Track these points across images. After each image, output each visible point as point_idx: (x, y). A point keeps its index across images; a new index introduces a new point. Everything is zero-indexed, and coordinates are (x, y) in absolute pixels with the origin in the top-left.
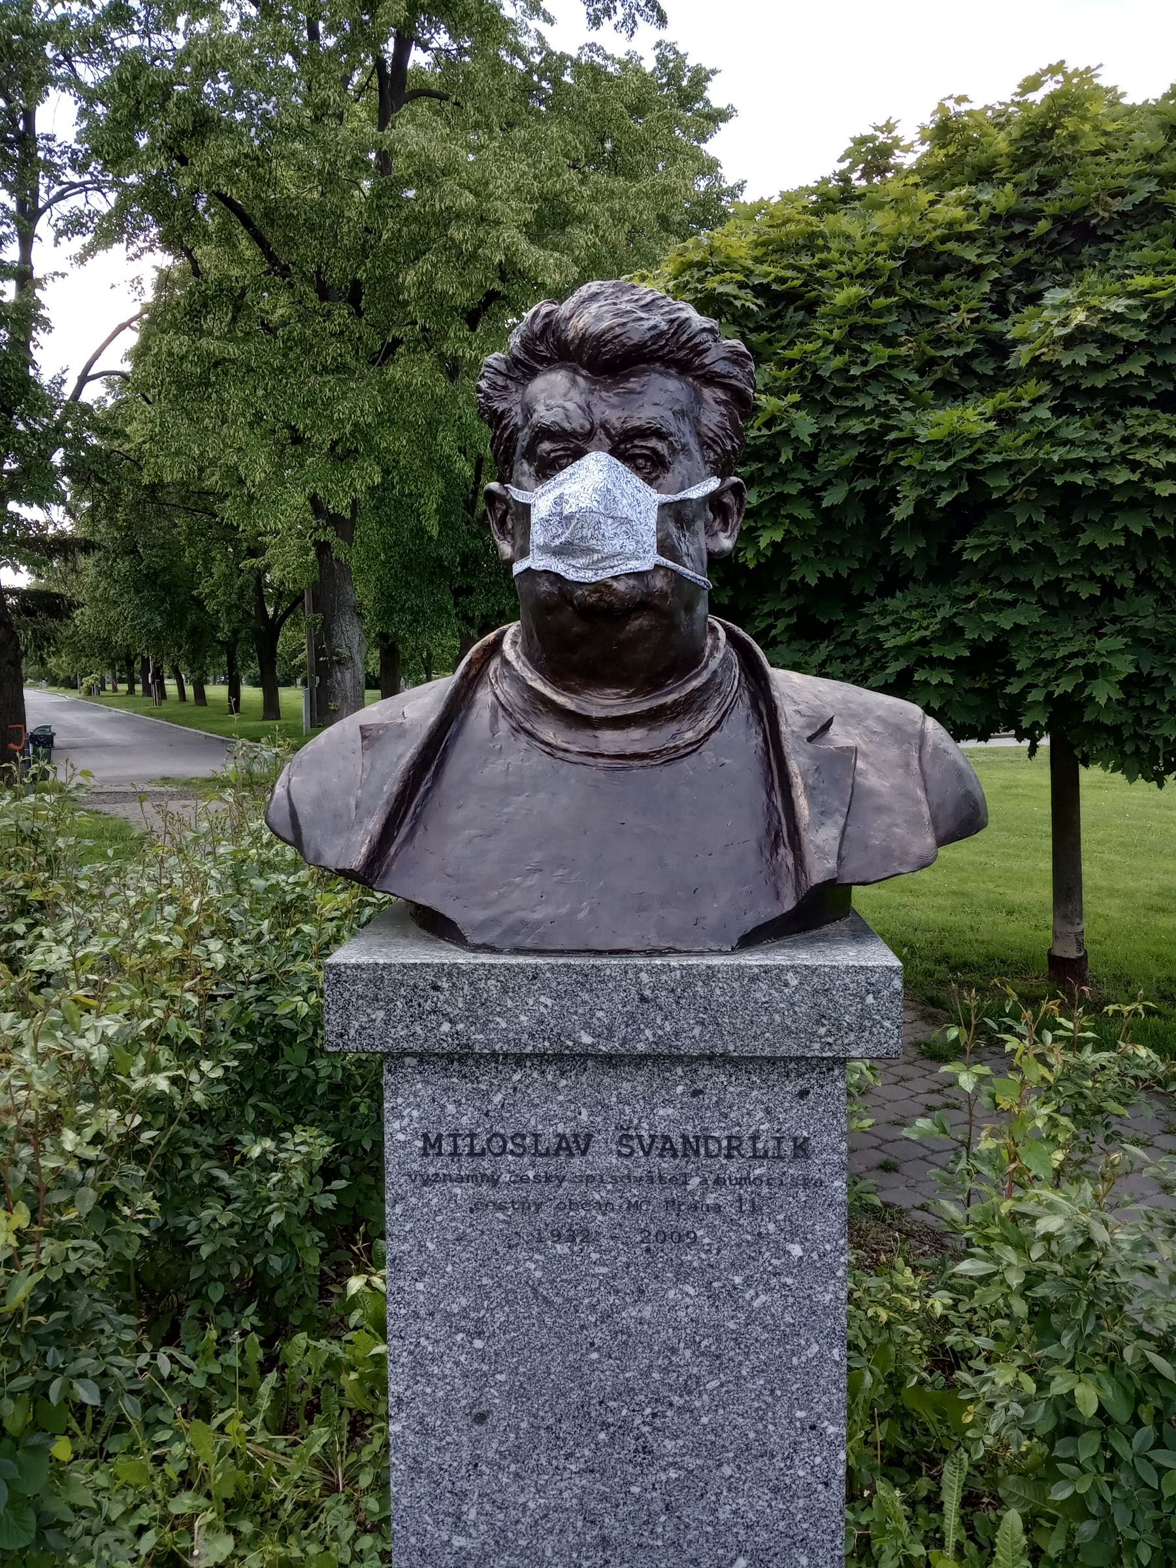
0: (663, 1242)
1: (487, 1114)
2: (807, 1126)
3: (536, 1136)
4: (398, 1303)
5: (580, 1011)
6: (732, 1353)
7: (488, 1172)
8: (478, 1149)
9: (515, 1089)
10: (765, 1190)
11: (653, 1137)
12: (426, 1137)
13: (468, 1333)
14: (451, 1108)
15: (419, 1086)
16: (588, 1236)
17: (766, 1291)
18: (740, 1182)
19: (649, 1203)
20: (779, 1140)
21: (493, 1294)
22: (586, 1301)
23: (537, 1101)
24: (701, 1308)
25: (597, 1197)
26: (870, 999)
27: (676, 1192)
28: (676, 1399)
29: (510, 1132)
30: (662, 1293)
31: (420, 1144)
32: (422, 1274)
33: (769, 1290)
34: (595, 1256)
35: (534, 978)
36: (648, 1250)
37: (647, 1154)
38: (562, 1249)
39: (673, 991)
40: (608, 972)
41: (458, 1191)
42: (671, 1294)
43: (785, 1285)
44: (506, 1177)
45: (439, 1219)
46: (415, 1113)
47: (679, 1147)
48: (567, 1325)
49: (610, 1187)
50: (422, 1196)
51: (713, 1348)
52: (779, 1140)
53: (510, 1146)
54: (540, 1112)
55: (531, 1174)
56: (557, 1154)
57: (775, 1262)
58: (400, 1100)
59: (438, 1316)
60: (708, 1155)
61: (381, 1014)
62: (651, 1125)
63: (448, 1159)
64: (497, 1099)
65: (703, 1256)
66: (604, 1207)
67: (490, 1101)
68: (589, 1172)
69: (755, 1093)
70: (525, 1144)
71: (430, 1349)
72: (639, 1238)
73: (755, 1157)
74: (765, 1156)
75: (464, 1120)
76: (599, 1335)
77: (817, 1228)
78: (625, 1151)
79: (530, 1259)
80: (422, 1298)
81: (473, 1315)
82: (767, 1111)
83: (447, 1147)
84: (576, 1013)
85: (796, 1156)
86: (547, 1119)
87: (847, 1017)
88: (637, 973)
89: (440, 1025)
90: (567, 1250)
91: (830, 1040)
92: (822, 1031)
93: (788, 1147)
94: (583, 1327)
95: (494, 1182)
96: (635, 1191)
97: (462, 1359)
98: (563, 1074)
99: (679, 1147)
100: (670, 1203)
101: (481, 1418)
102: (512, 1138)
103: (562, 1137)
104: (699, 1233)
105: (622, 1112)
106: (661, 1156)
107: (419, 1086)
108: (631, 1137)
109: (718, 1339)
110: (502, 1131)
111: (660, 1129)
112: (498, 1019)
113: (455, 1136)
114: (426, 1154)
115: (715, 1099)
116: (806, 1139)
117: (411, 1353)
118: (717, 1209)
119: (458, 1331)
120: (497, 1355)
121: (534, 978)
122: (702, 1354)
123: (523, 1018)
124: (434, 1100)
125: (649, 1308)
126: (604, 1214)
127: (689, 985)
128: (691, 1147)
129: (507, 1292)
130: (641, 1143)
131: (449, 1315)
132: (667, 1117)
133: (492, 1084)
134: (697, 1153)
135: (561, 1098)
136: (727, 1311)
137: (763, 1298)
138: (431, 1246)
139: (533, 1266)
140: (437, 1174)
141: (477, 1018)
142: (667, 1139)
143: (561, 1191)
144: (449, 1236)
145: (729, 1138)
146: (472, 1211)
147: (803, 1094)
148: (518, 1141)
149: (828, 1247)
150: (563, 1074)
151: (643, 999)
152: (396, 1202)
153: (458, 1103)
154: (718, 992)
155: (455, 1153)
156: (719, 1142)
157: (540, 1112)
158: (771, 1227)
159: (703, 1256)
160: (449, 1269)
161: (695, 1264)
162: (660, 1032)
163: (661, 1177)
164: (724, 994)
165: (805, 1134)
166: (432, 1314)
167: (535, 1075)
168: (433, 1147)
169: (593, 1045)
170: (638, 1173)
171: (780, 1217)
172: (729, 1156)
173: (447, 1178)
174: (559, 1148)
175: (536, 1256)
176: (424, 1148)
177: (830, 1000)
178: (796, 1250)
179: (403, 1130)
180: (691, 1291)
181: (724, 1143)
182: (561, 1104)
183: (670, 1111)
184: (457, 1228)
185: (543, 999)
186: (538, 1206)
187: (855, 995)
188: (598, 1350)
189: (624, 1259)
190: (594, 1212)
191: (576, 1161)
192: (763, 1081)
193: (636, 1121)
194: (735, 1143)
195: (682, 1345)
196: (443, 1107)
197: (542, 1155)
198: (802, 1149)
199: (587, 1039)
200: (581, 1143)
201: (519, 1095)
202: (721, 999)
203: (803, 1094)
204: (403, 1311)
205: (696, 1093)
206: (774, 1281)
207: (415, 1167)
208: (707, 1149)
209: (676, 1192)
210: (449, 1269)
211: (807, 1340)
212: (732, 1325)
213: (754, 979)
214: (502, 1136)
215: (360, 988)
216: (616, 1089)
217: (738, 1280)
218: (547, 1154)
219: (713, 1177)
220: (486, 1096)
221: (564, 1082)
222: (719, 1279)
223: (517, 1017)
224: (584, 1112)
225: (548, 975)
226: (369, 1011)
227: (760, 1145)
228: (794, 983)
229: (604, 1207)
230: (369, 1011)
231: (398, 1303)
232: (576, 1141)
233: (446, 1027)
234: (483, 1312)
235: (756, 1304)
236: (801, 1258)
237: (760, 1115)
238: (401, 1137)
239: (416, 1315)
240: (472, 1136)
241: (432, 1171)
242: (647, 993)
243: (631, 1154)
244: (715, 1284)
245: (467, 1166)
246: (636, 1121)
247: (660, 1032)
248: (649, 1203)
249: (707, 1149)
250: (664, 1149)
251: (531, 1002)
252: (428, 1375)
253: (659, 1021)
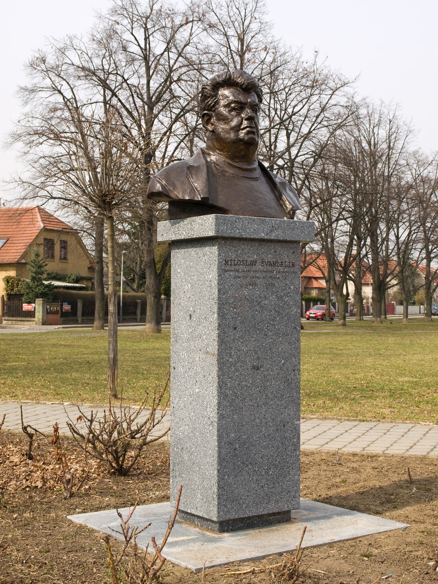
14: (230, 254)
16: (256, 284)
18: (283, 272)
27: (271, 274)
28: (272, 323)
32: (224, 293)
38: (251, 287)
44: (240, 270)
48: (252, 306)
61: (225, 227)
64: (239, 252)
66: (259, 278)
70: (244, 262)
76: (257, 308)
83: (229, 263)
86: (248, 257)
93: (291, 264)
95: (238, 271)
101: (235, 329)
113: (231, 260)
118: (279, 278)
128: (274, 264)
131: (230, 303)
132: (270, 257)
136: (280, 302)
142: (270, 262)
147: (294, 252)
151: (273, 227)
153: (232, 253)
170: (265, 270)
173: (230, 270)
178: (292, 287)
191: (254, 267)
198: (293, 265)
199: (263, 235)
200: (253, 263)
203: (294, 252)
205: (275, 252)
209: (271, 274)
213: (291, 223)
229: (259, 278)
233: (238, 231)
240: (234, 260)
245: (233, 268)
252: (225, 318)
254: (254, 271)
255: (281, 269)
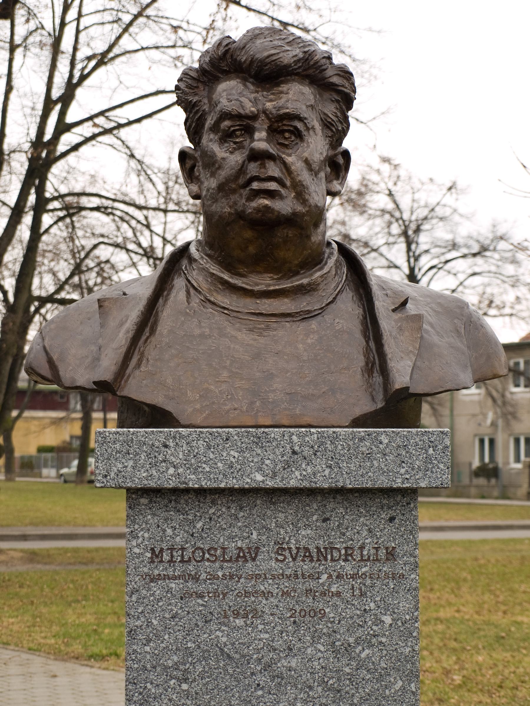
0: (304, 616)
1: (192, 535)
2: (395, 540)
3: (224, 549)
4: (133, 660)
5: (255, 460)
6: (348, 688)
7: (193, 573)
8: (186, 558)
9: (210, 519)
10: (368, 582)
11: (298, 549)
12: (152, 550)
13: (178, 679)
14: (169, 532)
15: (149, 517)
16: (256, 614)
17: (369, 647)
18: (353, 577)
19: (295, 591)
20: (377, 549)
21: (195, 653)
22: (255, 656)
23: (224, 526)
24: (328, 659)
25: (263, 588)
26: (431, 451)
27: (312, 584)
29: (207, 547)
30: (303, 650)
31: (149, 555)
32: (149, 641)
33: (371, 646)
34: (261, 627)
35: (227, 439)
36: (295, 622)
37: (294, 559)
38: (239, 622)
39: (312, 447)
40: (273, 435)
41: (173, 585)
42: (309, 651)
43: (381, 642)
44: (203, 576)
45: (160, 604)
46: (146, 535)
47: (315, 555)
49: (270, 581)
50: (149, 589)
51: (336, 685)
52: (377, 549)
53: (207, 556)
54: (227, 533)
55: (220, 574)
56: (237, 560)
57: (374, 627)
58: (136, 526)
59: (158, 669)
60: (332, 560)
61: (131, 463)
62: (297, 541)
63: (167, 565)
64: (199, 525)
65: (330, 625)
66: (267, 595)
67: (194, 527)
68: (257, 572)
69: (362, 519)
71: (153, 691)
72: (289, 615)
73: (362, 560)
74: (368, 560)
75: (178, 539)
76: (262, 679)
77: (401, 605)
78: (280, 558)
79: (219, 629)
80: (148, 657)
81: (181, 667)
82: (370, 531)
83: (166, 557)
84: (252, 461)
85: (387, 559)
86: (231, 538)
87: (417, 462)
88: (290, 436)
89: (168, 469)
90: (242, 623)
91: (408, 477)
92: (403, 471)
93: (382, 553)
94: (253, 674)
95: (196, 578)
96: (286, 584)
97: (174, 697)
98: (241, 509)
99: (315, 555)
100: (309, 591)
102: (208, 550)
103: (240, 549)
104: (327, 610)
105: (278, 533)
106: (303, 561)
107: (149, 517)
108: (284, 549)
109: (339, 680)
110: (202, 546)
111: (303, 543)
112: (204, 466)
113: (172, 549)
114: (153, 562)
115: (337, 523)
116: (394, 548)
117: (140, 694)
118: (338, 594)
119: (172, 678)
120: (197, 693)
121: (227, 439)
122: (329, 690)
123: (219, 464)
124: (158, 526)
125: (295, 660)
126: (267, 599)
127: (322, 443)
129: (204, 652)
130: (290, 553)
132: (307, 536)
133: (196, 516)
134: (326, 559)
135: (240, 524)
136: (344, 661)
137: (367, 651)
138: (155, 622)
139: (220, 634)
140: (160, 575)
141: (191, 465)
142: (307, 549)
143: (239, 585)
144: (167, 615)
145: (346, 548)
146: (182, 598)
147: (392, 519)
148: (212, 552)
149: (408, 617)
150: (241, 509)
151: (294, 453)
152: (132, 593)
154: (340, 447)
155: (171, 561)
156: (340, 551)
157: (227, 533)
158: (372, 605)
159: (330, 625)
160: (166, 637)
161: (325, 631)
162: (304, 473)
163: (303, 575)
164: (343, 448)
165: (393, 545)
166: (155, 667)
167: (224, 510)
168: (157, 557)
169: (263, 482)
170: (288, 572)
171: (378, 599)
172: (346, 560)
173: (167, 577)
174: (239, 556)
175: (223, 628)
176: (152, 558)
177: (407, 452)
178: (388, 620)
179: (138, 546)
180: (322, 648)
181: (343, 552)
182: (240, 528)
183: (309, 532)
184: (172, 610)
185: (232, 453)
186: (225, 595)
187: (422, 449)
188: (262, 689)
189: (280, 629)
190: (260, 598)
191: (249, 565)
192: (367, 512)
193: (287, 539)
194: (350, 552)
195: (316, 684)
196: (164, 531)
197: (227, 561)
198: (391, 555)
199: (259, 477)
200: (251, 554)
201: (213, 522)
202: (342, 452)
203: (392, 519)
204: (136, 666)
205: (325, 520)
206: (374, 640)
207: (146, 570)
208: (332, 556)
209: (312, 584)
210: (166, 637)
211: (395, 678)
212: (347, 670)
213: (362, 439)
214: (202, 549)
215: (118, 446)
216: (275, 518)
217: (351, 640)
218: (230, 561)
219: (336, 574)
220: (192, 523)
221: (242, 514)
222: (339, 640)
223: (216, 464)
224: (255, 534)
225: (236, 437)
226: (123, 461)
227: (365, 553)
228: (386, 441)
229: (267, 595)
230: (123, 461)
231: (133, 660)
232: (249, 552)
233: (171, 471)
234: (188, 665)
235: (363, 655)
236: (391, 625)
237: (365, 533)
238: (137, 550)
239: (145, 668)
240: (183, 549)
241: (156, 572)
242: (297, 448)
243: (284, 560)
244: (337, 643)
246: (287, 539)
247: (304, 473)
248: (295, 591)
249: (332, 556)
250: (305, 556)
251: (225, 454)
253: (304, 466)
254: (250, 577)
255: (348, 568)
